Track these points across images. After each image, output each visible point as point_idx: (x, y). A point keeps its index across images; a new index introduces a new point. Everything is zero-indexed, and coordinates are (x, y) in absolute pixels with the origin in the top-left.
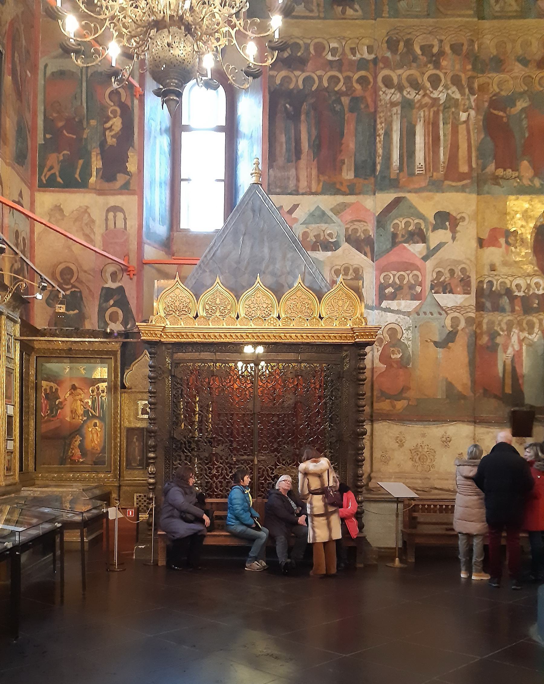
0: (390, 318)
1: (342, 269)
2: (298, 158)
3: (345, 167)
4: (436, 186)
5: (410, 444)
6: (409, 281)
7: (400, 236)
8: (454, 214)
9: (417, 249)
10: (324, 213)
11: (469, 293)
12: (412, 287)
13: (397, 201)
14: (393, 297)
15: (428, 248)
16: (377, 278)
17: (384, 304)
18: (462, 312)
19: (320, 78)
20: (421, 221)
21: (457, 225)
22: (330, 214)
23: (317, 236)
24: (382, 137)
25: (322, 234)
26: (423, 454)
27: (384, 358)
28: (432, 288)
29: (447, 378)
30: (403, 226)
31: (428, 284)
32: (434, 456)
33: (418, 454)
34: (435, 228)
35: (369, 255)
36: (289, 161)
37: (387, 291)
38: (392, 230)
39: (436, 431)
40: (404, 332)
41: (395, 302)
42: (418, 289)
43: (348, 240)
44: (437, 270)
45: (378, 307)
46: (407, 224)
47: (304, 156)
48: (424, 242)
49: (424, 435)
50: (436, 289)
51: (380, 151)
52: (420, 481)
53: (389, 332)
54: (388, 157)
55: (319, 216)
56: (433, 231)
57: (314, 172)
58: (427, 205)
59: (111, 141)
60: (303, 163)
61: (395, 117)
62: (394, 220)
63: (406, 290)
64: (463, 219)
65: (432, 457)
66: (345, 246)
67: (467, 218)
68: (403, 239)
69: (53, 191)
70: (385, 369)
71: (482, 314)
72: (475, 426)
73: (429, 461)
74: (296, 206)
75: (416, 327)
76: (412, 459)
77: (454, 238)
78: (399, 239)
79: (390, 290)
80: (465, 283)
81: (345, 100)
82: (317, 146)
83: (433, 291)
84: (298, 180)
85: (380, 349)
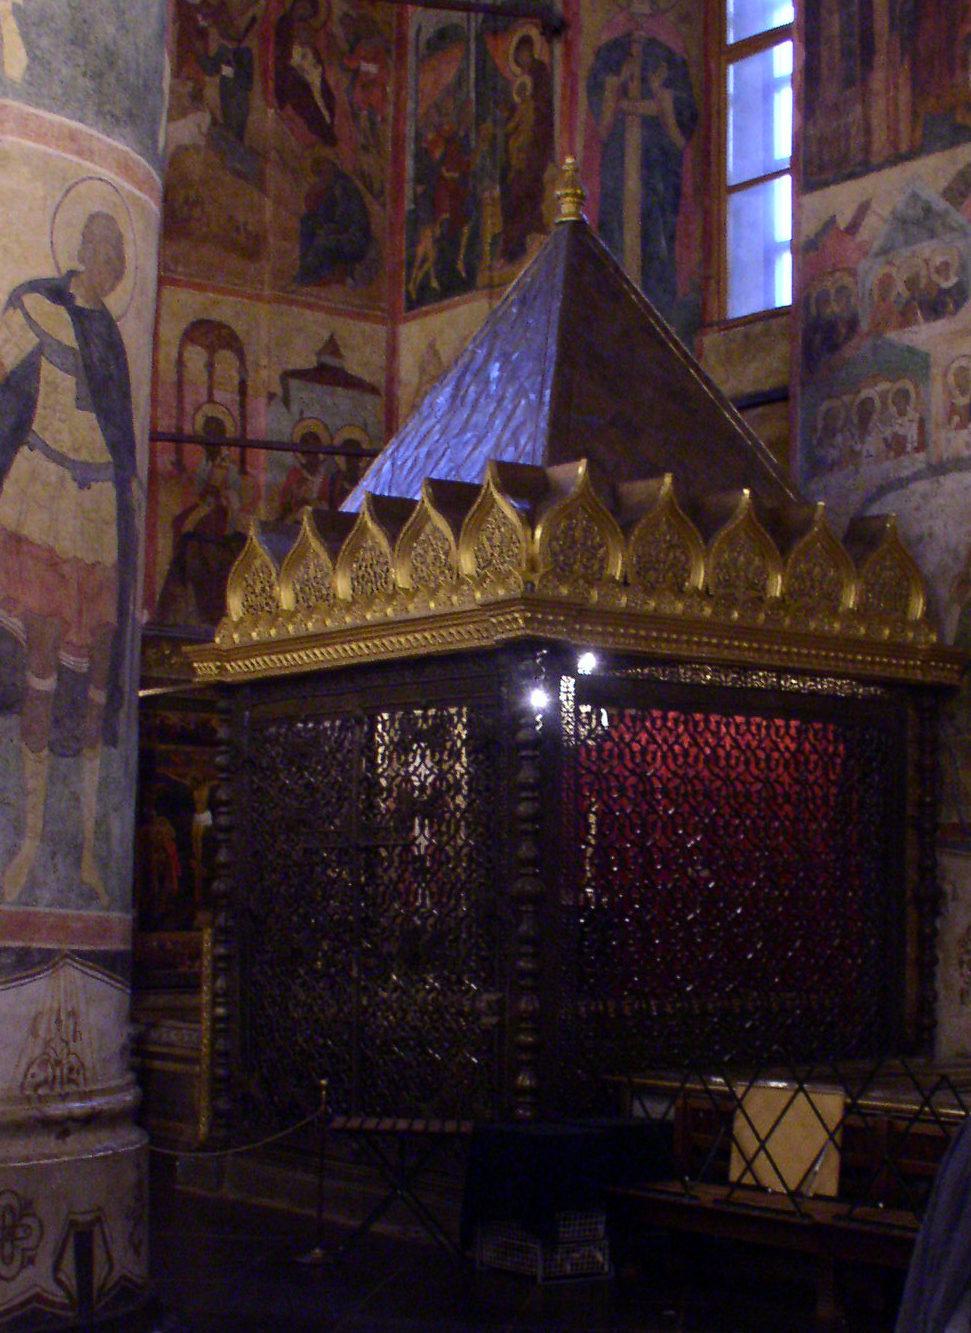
10: (928, 210)
22: (941, 205)
23: (912, 283)
25: (924, 272)
36: (849, 83)
47: (880, 59)
55: (919, 221)
57: (904, 96)
59: (517, 161)
60: (878, 80)
69: (427, 314)
74: (864, 209)
84: (868, 131)
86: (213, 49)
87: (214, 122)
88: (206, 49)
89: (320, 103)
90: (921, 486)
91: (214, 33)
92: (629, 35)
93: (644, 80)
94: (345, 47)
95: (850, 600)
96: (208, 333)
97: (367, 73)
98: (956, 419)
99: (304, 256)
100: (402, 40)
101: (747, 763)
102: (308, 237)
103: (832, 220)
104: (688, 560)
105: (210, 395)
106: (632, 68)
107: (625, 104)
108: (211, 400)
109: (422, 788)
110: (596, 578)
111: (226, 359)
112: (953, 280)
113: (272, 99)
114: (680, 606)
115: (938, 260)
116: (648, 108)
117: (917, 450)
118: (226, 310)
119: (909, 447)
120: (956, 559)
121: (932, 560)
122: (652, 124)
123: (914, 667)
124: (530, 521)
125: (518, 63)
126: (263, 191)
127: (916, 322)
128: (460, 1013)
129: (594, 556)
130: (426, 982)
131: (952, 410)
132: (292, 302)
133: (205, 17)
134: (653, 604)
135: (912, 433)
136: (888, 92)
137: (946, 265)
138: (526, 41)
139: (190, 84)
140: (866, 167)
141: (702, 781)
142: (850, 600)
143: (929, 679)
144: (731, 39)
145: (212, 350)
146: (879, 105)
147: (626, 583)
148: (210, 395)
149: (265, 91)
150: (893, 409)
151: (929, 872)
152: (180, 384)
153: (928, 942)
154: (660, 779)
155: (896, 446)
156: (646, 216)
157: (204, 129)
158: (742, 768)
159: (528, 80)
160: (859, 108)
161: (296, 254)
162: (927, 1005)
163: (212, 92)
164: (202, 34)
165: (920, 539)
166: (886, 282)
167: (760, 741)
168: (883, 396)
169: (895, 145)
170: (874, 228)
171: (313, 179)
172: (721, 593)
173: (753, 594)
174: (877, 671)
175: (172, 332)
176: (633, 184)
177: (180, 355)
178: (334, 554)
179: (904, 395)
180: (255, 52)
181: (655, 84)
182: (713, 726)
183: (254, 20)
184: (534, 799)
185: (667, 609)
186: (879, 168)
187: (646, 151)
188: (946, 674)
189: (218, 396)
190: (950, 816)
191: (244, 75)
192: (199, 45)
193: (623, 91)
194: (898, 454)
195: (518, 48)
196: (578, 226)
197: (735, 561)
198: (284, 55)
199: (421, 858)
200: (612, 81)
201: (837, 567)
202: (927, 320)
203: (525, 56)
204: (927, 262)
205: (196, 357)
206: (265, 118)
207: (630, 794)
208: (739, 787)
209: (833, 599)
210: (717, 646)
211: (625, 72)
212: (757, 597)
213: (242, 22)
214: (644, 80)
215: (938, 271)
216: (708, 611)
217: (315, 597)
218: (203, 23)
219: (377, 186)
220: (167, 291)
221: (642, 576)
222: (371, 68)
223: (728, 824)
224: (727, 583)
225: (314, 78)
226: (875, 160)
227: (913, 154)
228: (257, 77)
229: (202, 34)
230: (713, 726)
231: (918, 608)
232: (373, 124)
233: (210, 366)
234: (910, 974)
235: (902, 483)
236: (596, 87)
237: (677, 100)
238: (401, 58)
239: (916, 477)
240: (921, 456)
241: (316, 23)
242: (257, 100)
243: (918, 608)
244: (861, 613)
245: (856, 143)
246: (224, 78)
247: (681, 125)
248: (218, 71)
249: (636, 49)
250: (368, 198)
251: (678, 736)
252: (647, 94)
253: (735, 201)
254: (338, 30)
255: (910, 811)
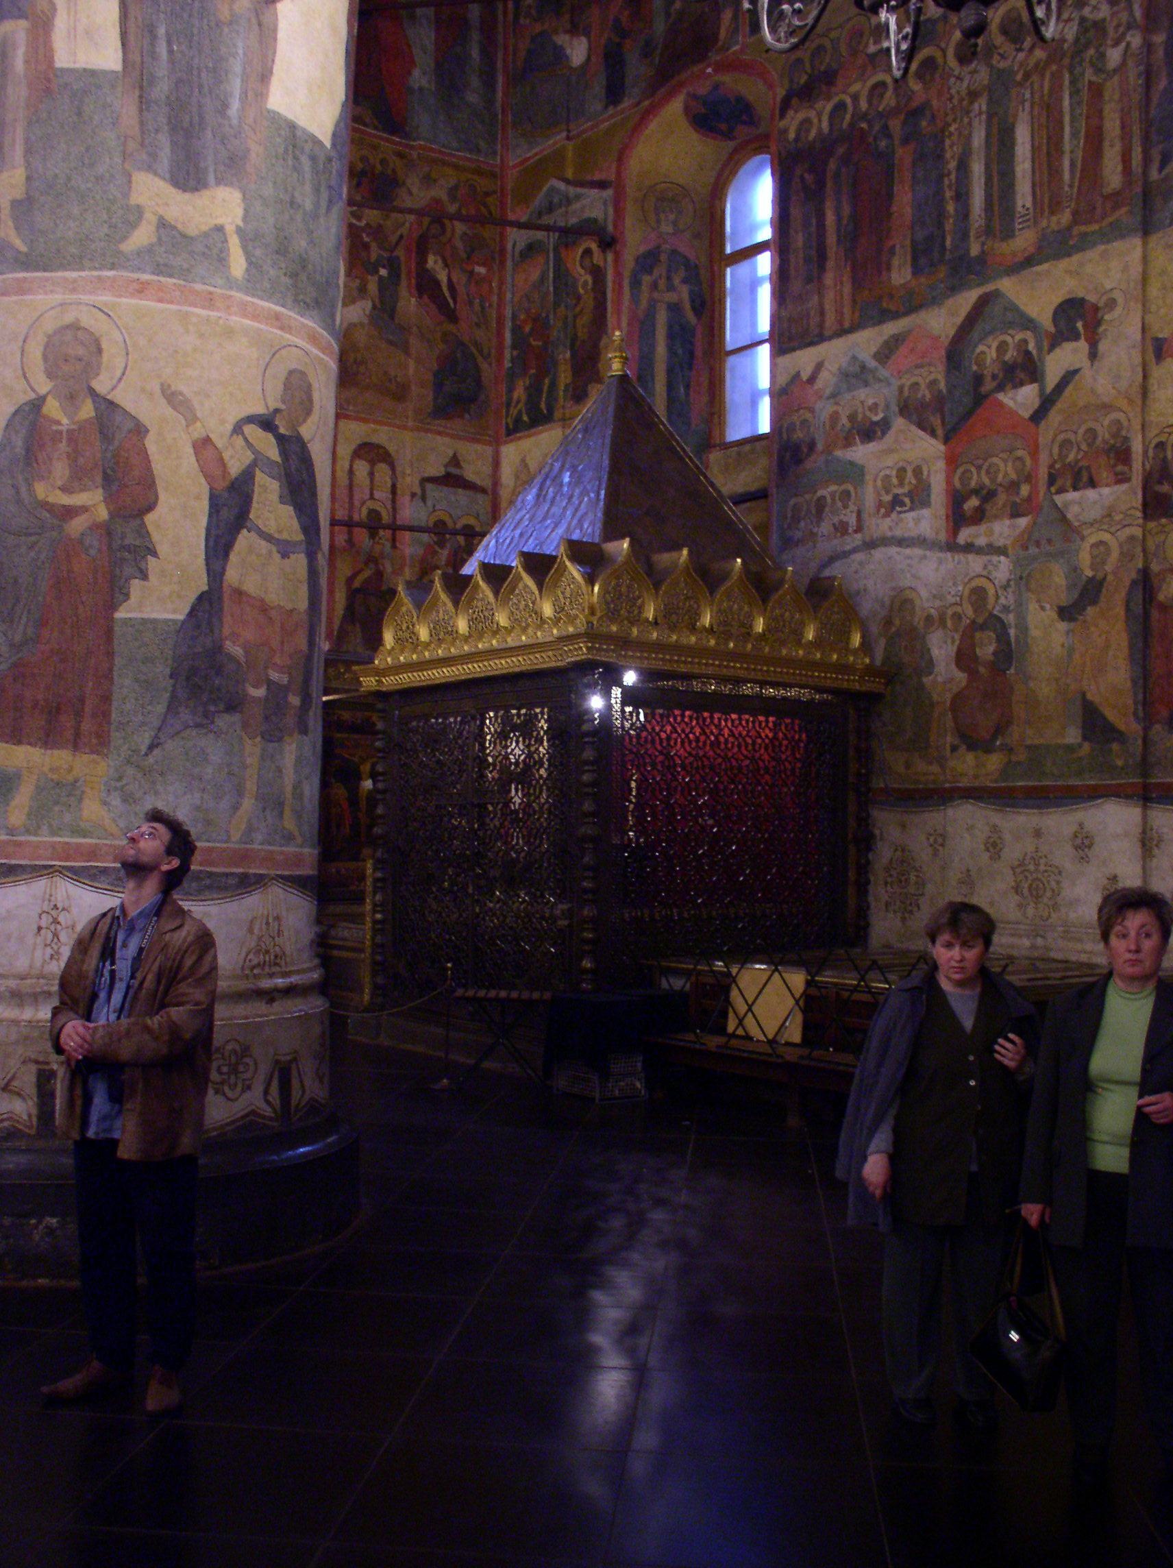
0: (975, 563)
1: (894, 473)
2: (822, 267)
3: (896, 262)
4: (1056, 247)
5: (1013, 852)
6: (1006, 474)
7: (989, 378)
8: (1092, 298)
9: (1024, 398)
10: (863, 367)
11: (1128, 480)
12: (1014, 486)
13: (984, 302)
14: (979, 517)
15: (1042, 389)
16: (949, 481)
17: (964, 536)
18: (1113, 529)
19: (855, 98)
20: (1028, 335)
21: (1099, 323)
22: (872, 364)
23: (852, 418)
24: (953, 177)
25: (860, 410)
26: (1037, 879)
27: (964, 658)
28: (1052, 480)
29: (1084, 694)
30: (994, 355)
31: (1043, 473)
32: (1058, 883)
33: (1026, 877)
34: (1056, 341)
35: (940, 432)
36: (809, 280)
37: (966, 507)
38: (975, 368)
39: (1060, 823)
40: (1000, 593)
41: (983, 528)
42: (1025, 490)
43: (905, 409)
44: (1062, 437)
45: (952, 546)
46: (1002, 348)
47: (830, 264)
48: (1034, 380)
49: (1038, 833)
50: (1059, 483)
51: (951, 208)
52: (1026, 943)
53: (974, 598)
54: (965, 214)
55: (857, 375)
56: (1050, 351)
57: (847, 289)
58: (1037, 295)
59: (582, 334)
60: (829, 279)
61: (976, 123)
62: (976, 346)
63: (1002, 498)
64: (1112, 304)
65: (1053, 884)
66: (899, 423)
67: (1120, 301)
68: (995, 384)
69: (520, 438)
70: (964, 684)
71: (1164, 526)
72: (1145, 807)
73: (1049, 894)
74: (819, 366)
75: (1021, 578)
76: (1017, 889)
77: (1093, 355)
78: (989, 385)
79: (973, 502)
80: (1122, 454)
81: (895, 125)
82: (850, 239)
83: (1053, 489)
84: (822, 313)
85: (957, 637)
86: (374, 257)
87: (374, 307)
88: (369, 257)
89: (447, 294)
90: (859, 557)
91: (374, 246)
92: (659, 247)
93: (669, 278)
94: (464, 256)
95: (810, 635)
96: (370, 452)
97: (479, 274)
98: (883, 510)
99: (435, 399)
100: (502, 251)
101: (739, 746)
102: (438, 386)
103: (798, 374)
104: (699, 606)
105: (372, 494)
106: (661, 270)
107: (656, 295)
108: (372, 497)
109: (517, 764)
110: (636, 620)
111: (382, 468)
112: (881, 415)
113: (414, 291)
114: (693, 639)
115: (870, 402)
116: (671, 297)
117: (856, 532)
118: (382, 436)
119: (850, 530)
120: (883, 605)
121: (866, 607)
122: (674, 308)
123: (854, 681)
124: (591, 581)
125: (583, 267)
126: (408, 354)
127: (855, 444)
128: (543, 918)
129: (635, 604)
130: (519, 897)
131: (880, 505)
132: (427, 431)
133: (368, 235)
134: (675, 637)
135: (852, 520)
136: (836, 284)
137: (876, 405)
138: (588, 252)
139: (358, 281)
140: (821, 338)
141: (708, 759)
142: (810, 635)
143: (864, 689)
144: (728, 250)
145: (373, 463)
146: (830, 296)
147: (656, 623)
148: (372, 494)
149: (409, 286)
150: (839, 504)
151: (864, 821)
152: (351, 487)
153: (864, 869)
154: (679, 757)
155: (842, 529)
156: (670, 371)
157: (367, 312)
158: (736, 750)
159: (589, 279)
160: (816, 298)
161: (430, 398)
162: (863, 912)
163: (373, 287)
164: (366, 247)
165: (858, 593)
166: (834, 417)
167: (749, 731)
168: (833, 495)
169: (841, 323)
170: (826, 379)
171: (442, 346)
172: (721, 630)
173: (744, 630)
174: (829, 683)
175: (345, 451)
176: (661, 350)
177: (351, 466)
178: (456, 603)
179: (847, 494)
180: (402, 259)
181: (676, 281)
182: (716, 721)
183: (401, 237)
184: (593, 771)
185: (684, 641)
186: (830, 338)
187: (670, 327)
188: (874, 685)
189: (377, 495)
190: (878, 783)
191: (395, 274)
192: (364, 254)
193: (654, 286)
194: (843, 535)
195: (582, 257)
196: (624, 378)
197: (731, 608)
198: (422, 261)
199: (516, 812)
200: (647, 279)
201: (801, 612)
202: (862, 443)
203: (587, 262)
204: (862, 402)
205: (362, 468)
206: (409, 304)
207: (659, 768)
208: (734, 763)
209: (798, 634)
210: (719, 666)
211: (656, 273)
212: (747, 633)
213: (393, 239)
214: (669, 278)
215: (870, 409)
216: (712, 642)
217: (443, 633)
218: (366, 239)
219: (486, 351)
220: (342, 423)
221: (668, 618)
222: (481, 270)
223: (726, 788)
224: (725, 623)
225: (443, 277)
226: (827, 333)
227: (852, 329)
228: (403, 276)
229: (366, 247)
230: (716, 721)
231: (856, 640)
232: (483, 308)
233: (371, 474)
234: (851, 890)
235: (846, 554)
236: (636, 283)
237: (691, 292)
238: (502, 263)
239: (855, 550)
240: (859, 536)
241: (444, 239)
242: (403, 291)
243: (856, 640)
244: (818, 643)
245: (814, 321)
246: (381, 278)
247: (693, 308)
248: (377, 272)
249: (663, 257)
250: (480, 360)
251: (692, 728)
252: (671, 288)
253: (731, 361)
254: (459, 244)
255: (851, 779)
